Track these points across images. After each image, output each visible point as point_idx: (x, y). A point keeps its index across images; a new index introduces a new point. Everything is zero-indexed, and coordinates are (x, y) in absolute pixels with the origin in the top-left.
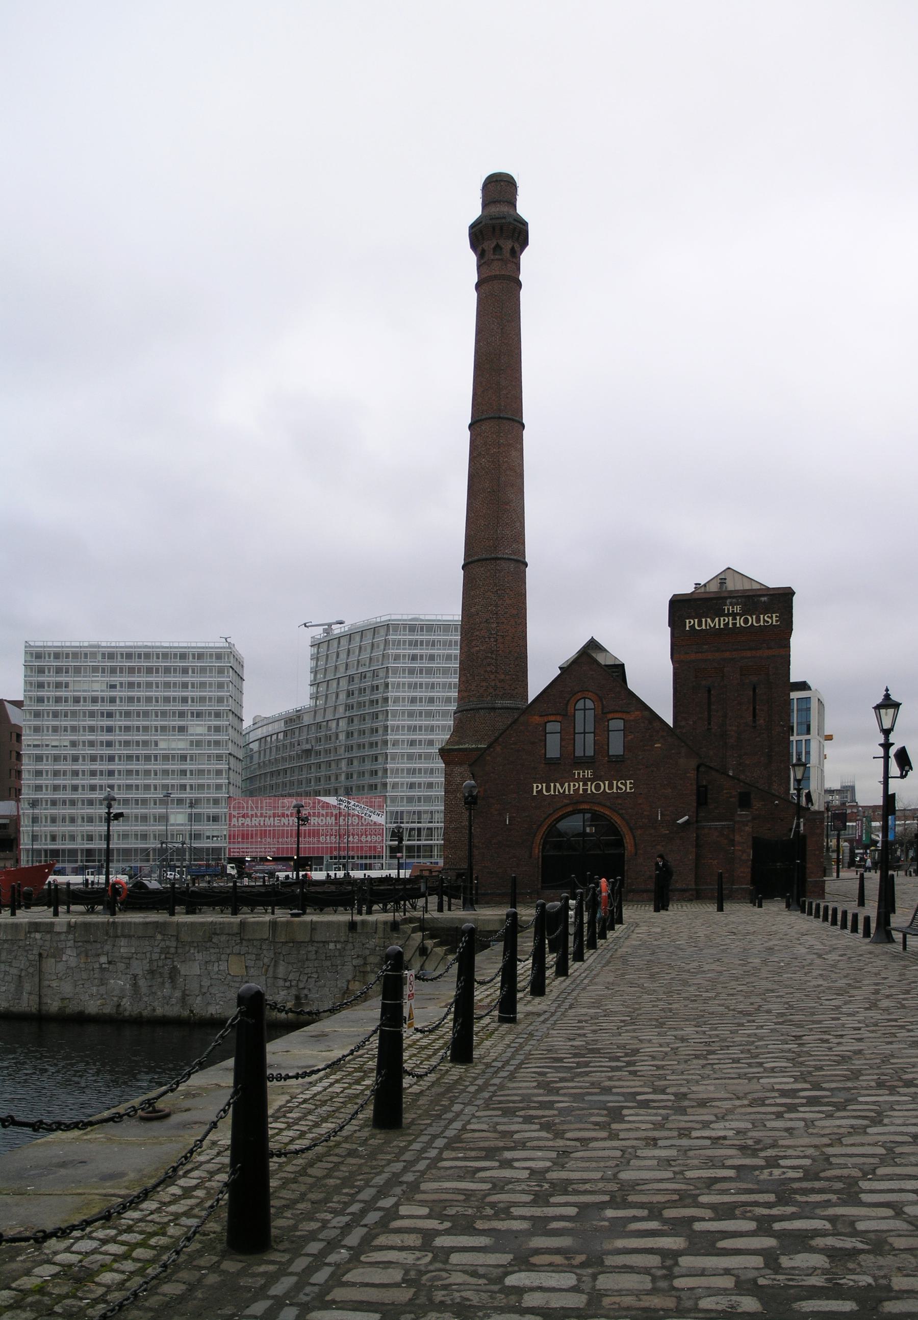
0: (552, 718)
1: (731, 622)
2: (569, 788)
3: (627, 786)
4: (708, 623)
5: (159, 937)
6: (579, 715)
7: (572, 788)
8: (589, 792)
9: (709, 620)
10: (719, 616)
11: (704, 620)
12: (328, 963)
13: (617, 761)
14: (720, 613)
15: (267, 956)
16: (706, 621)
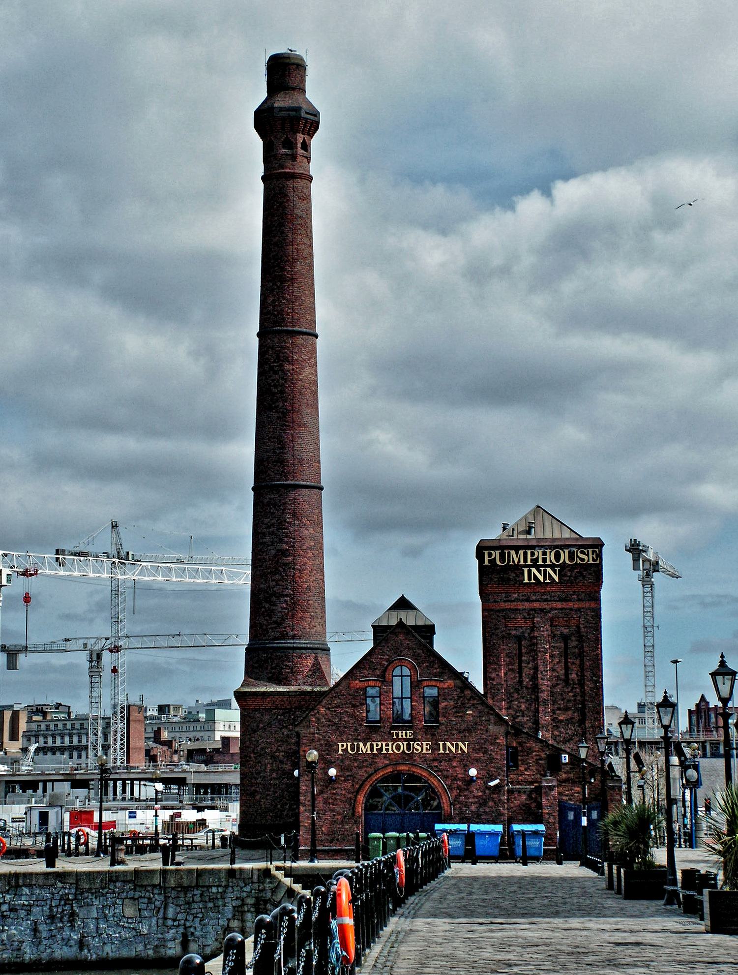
5: (59, 885)
6: (397, 681)
12: (211, 905)
15: (159, 899)
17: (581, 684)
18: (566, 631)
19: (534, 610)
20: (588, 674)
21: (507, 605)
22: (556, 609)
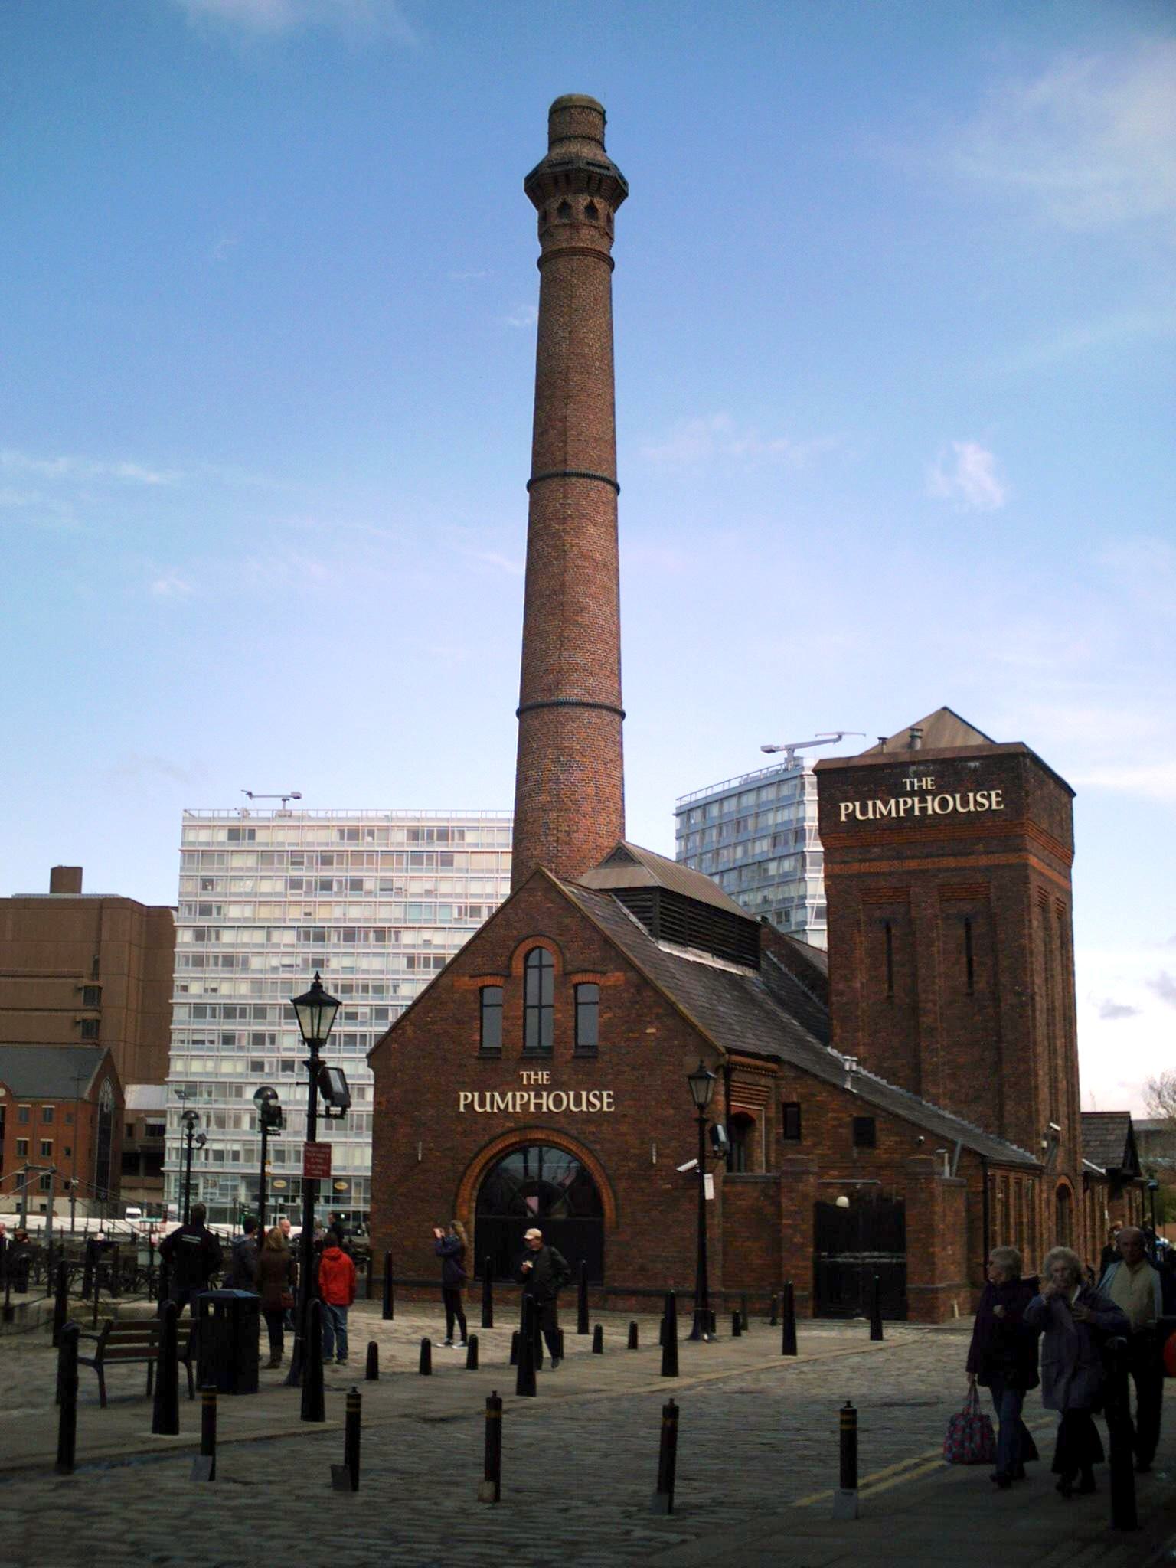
0: (488, 980)
1: (917, 806)
2: (514, 1101)
3: (603, 1101)
4: (879, 809)
7: (518, 1102)
8: (545, 1109)
9: (879, 803)
10: (896, 797)
11: (870, 803)
13: (587, 1055)
14: (899, 792)
16: (874, 805)
17: (996, 999)
18: (967, 907)
19: (910, 873)
20: (1004, 979)
21: (865, 867)
22: (948, 870)
